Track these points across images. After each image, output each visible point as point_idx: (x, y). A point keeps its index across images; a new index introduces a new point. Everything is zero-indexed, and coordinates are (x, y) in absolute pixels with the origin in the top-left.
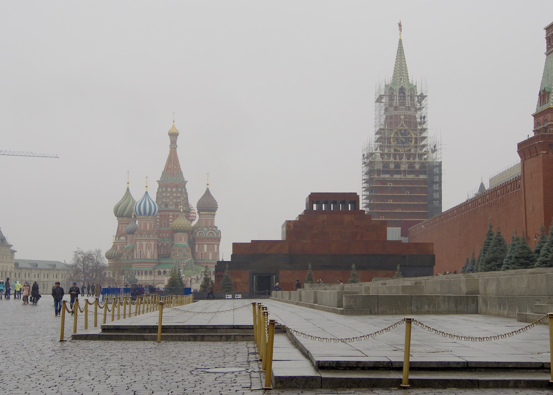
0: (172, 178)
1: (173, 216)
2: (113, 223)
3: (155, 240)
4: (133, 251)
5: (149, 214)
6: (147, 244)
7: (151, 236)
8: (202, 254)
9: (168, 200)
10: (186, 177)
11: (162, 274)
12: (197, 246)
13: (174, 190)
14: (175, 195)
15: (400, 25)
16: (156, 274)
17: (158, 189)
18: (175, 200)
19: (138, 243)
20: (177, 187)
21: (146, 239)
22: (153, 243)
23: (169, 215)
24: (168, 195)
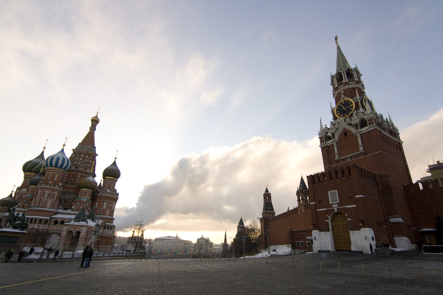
0: (87, 150)
1: (81, 176)
2: (18, 179)
3: (59, 191)
4: (31, 200)
5: (61, 167)
6: (50, 194)
7: (57, 186)
8: (100, 210)
9: (79, 163)
10: (98, 151)
11: (59, 223)
12: (97, 202)
13: (87, 157)
14: (86, 160)
15: (336, 39)
16: (52, 223)
17: (72, 155)
18: (85, 165)
19: (39, 191)
20: (89, 155)
21: (50, 189)
22: (56, 194)
23: (77, 175)
24: (81, 159)
